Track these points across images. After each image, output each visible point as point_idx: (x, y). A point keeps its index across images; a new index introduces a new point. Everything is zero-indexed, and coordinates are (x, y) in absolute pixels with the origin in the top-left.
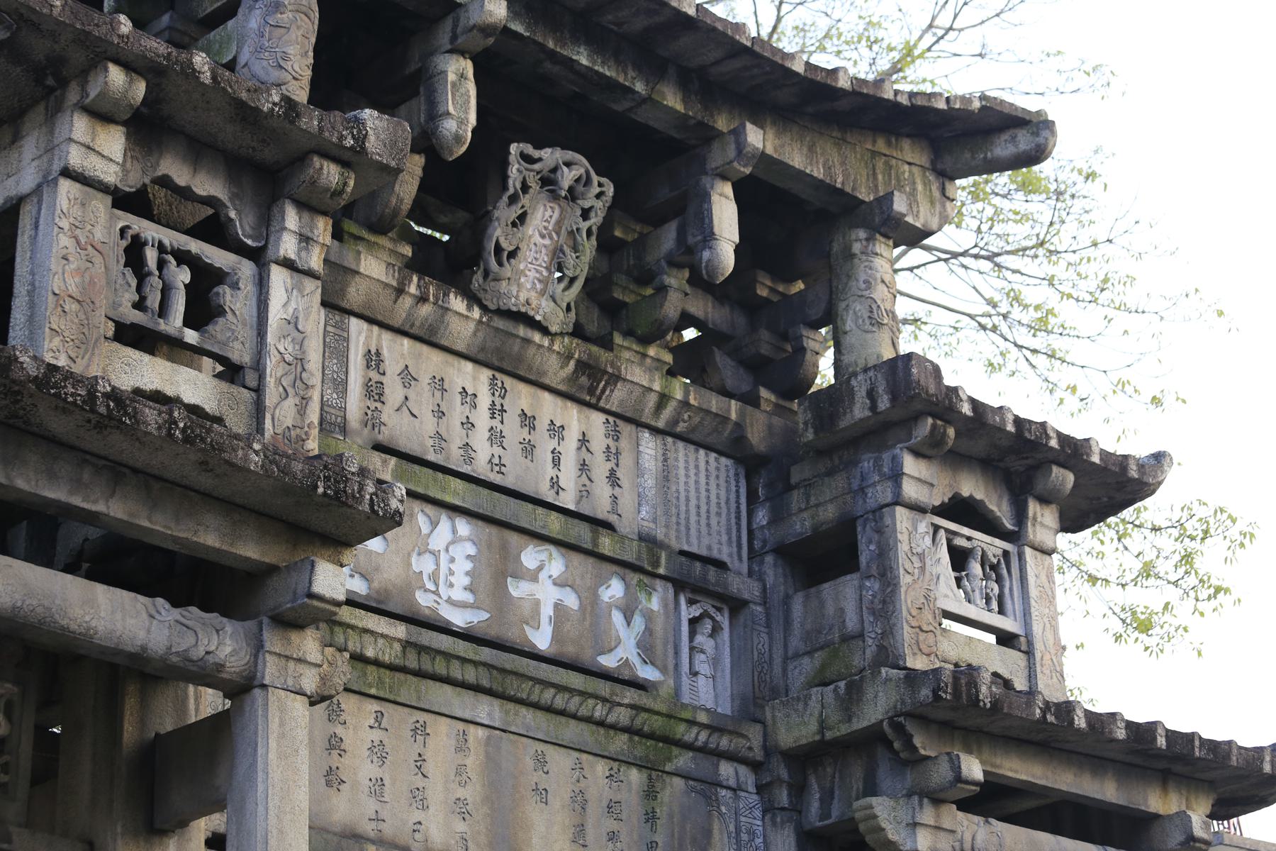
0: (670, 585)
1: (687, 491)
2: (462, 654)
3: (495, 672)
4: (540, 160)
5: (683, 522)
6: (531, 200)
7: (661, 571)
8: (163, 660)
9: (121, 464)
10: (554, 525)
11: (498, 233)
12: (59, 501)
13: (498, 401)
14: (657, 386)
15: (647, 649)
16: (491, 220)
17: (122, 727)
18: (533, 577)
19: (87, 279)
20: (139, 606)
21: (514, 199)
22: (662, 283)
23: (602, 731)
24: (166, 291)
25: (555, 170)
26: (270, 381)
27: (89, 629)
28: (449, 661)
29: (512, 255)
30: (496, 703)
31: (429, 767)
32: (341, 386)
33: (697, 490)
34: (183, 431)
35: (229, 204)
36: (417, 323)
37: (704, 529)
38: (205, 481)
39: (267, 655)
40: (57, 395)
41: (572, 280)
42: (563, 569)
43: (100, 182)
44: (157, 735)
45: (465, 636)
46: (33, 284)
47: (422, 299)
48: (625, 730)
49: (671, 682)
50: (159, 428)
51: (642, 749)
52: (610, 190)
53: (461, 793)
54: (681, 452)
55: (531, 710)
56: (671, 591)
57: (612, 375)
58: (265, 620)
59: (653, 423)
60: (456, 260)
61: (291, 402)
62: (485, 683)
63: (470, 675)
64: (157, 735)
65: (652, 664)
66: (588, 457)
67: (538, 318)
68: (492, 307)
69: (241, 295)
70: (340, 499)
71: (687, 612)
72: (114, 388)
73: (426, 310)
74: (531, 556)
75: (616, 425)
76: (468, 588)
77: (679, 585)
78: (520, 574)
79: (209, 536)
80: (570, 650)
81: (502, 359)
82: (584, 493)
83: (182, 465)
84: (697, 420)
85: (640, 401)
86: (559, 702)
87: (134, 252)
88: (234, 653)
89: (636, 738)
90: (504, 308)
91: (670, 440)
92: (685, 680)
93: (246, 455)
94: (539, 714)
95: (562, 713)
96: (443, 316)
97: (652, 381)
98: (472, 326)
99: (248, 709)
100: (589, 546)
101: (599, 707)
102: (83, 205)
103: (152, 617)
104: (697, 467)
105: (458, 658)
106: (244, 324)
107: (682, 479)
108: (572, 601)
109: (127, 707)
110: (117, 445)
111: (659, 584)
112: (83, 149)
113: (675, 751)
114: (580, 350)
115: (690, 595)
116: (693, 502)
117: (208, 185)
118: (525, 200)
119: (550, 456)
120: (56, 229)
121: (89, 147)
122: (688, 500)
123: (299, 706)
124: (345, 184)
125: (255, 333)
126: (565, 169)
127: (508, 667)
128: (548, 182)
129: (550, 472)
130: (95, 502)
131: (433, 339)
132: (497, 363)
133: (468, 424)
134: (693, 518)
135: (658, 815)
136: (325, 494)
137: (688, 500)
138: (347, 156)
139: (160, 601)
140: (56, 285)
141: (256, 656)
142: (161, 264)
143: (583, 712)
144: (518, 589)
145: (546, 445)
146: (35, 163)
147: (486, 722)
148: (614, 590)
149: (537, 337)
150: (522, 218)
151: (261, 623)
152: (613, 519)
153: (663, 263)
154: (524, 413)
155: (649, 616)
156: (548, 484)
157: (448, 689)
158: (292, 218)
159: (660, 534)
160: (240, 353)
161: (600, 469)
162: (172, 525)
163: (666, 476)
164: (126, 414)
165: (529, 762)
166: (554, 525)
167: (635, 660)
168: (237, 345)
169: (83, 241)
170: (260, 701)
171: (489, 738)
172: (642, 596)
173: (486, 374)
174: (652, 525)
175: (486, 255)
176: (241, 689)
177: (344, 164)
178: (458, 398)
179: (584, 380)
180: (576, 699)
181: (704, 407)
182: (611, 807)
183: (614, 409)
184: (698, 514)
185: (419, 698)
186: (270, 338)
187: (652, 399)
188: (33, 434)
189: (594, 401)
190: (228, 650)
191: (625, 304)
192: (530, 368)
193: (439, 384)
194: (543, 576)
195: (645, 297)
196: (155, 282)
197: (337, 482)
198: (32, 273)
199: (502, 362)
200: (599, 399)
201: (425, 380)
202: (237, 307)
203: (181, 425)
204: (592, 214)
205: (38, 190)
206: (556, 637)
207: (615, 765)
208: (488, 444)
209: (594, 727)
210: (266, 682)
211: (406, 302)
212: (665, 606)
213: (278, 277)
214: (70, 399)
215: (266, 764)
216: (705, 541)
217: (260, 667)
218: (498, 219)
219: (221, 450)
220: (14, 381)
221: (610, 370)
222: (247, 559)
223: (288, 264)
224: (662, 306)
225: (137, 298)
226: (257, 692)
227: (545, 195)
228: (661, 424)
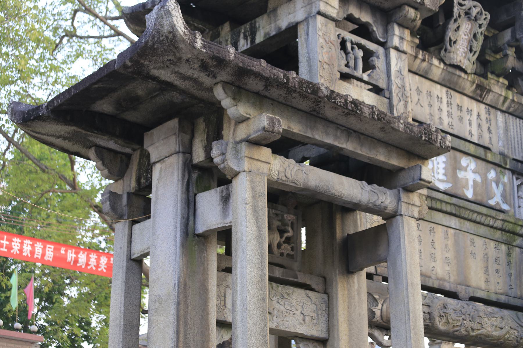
0: (510, 172)
1: (514, 135)
2: (446, 200)
3: (457, 207)
4: (465, 5)
5: (513, 147)
6: (461, 21)
7: (508, 167)
8: (366, 206)
9: (350, 129)
10: (472, 149)
11: (450, 34)
12: (330, 144)
13: (449, 100)
14: (503, 94)
15: (504, 196)
16: (447, 29)
17: (336, 231)
18: (465, 169)
19: (330, 55)
20: (357, 184)
21: (456, 20)
22: (506, 53)
23: (492, 230)
24: (356, 59)
25: (470, 9)
26: (394, 95)
27: (341, 194)
28: (441, 203)
29: (455, 42)
30: (457, 219)
31: (436, 245)
33: (517, 134)
34: (377, 116)
35: (373, 25)
36: (421, 70)
37: (520, 150)
38: (380, 135)
39: (402, 203)
40: (335, 102)
41: (475, 52)
42: (475, 166)
43: (331, 17)
44: (348, 234)
45: (445, 193)
46: (309, 57)
47: (424, 60)
48: (500, 229)
49: (513, 210)
50: (369, 115)
51: (506, 237)
52: (489, 17)
53: (447, 255)
54: (511, 119)
55: (469, 222)
56: (511, 174)
57: (488, 90)
58: (401, 189)
59: (501, 108)
61: (402, 103)
62: (454, 212)
63: (448, 208)
64: (348, 234)
65: (506, 203)
66: (480, 122)
67: (464, 67)
68: (448, 63)
69: (380, 60)
70: (430, 142)
71: (516, 183)
72: (353, 99)
73: (425, 64)
74: (465, 161)
75: (489, 109)
76: (445, 174)
77: (513, 172)
78: (461, 168)
79: (381, 156)
80: (479, 198)
81: (450, 84)
82: (480, 137)
83: (374, 129)
84: (517, 107)
85: (498, 100)
86: (478, 219)
87: (343, 44)
88: (391, 202)
89: (503, 233)
90: (452, 63)
91: (507, 115)
92: (517, 209)
93: (398, 125)
94: (472, 224)
95: (479, 223)
96: (430, 67)
97: (502, 92)
98: (440, 71)
99: (394, 224)
100: (483, 157)
101: (491, 220)
102: (326, 26)
103: (362, 188)
104: (516, 125)
105: (445, 202)
106: (382, 72)
107: (512, 130)
108: (479, 179)
109: (337, 223)
110: (352, 122)
111: (507, 172)
112: (325, 4)
113: (516, 237)
114: (478, 80)
115: (517, 176)
116: (516, 139)
117: (365, 17)
118: (459, 21)
119: (468, 122)
120: (318, 36)
121: (327, 3)
122: (514, 138)
123: (413, 223)
124: (417, 17)
125: (386, 76)
126: (474, 8)
127: (461, 205)
128: (467, 13)
129: (468, 128)
130: (342, 144)
131: (427, 76)
132: (448, 85)
133: (440, 110)
134: (516, 146)
135: (512, 262)
136: (425, 140)
137: (514, 138)
138: (417, 6)
139: (364, 182)
140: (320, 58)
141: (398, 203)
142: (353, 49)
143: (486, 222)
144: (461, 175)
145: (466, 117)
146: (303, 9)
147: (454, 227)
148: (492, 174)
149: (463, 75)
150: (458, 28)
151: (399, 190)
152: (490, 146)
153: (506, 45)
154: (458, 105)
155: (504, 185)
156: (468, 133)
157: (441, 214)
158: (397, 30)
159: (506, 152)
160: (382, 84)
161: (485, 127)
162: (369, 152)
163: (506, 129)
164: (358, 109)
165: (469, 243)
166: (472, 149)
167: (501, 202)
168: (381, 81)
169: (327, 40)
170: (400, 221)
171: (455, 233)
172: (501, 177)
173: (444, 89)
174: (503, 149)
175: (446, 43)
176: (390, 217)
177: (416, 9)
178: (436, 99)
179: (479, 92)
180: (484, 218)
181: (520, 102)
182: (497, 259)
183: (488, 103)
184: (518, 144)
185: (431, 218)
186: (393, 78)
187: (502, 99)
188: (319, 117)
189: (481, 100)
190: (389, 201)
191: (489, 61)
192: (460, 87)
193: (430, 94)
194: (468, 169)
195: (497, 59)
196: (351, 56)
197: (429, 135)
198: (308, 53)
199: (450, 85)
200: (483, 99)
201: (425, 92)
202: (379, 65)
203: (376, 113)
204: (483, 26)
205: (306, 19)
206: (475, 193)
207: (497, 243)
208: (447, 117)
209: (489, 228)
210: (402, 213)
211: (418, 61)
212: (509, 180)
213: (393, 53)
214: (339, 104)
215: (405, 245)
216: (521, 155)
217: (399, 208)
218: (450, 28)
219: (390, 123)
220: (320, 97)
221: (488, 88)
222: (394, 165)
223: (396, 49)
224: (506, 62)
225: (346, 62)
226: (398, 217)
227: (466, 19)
228: (504, 109)
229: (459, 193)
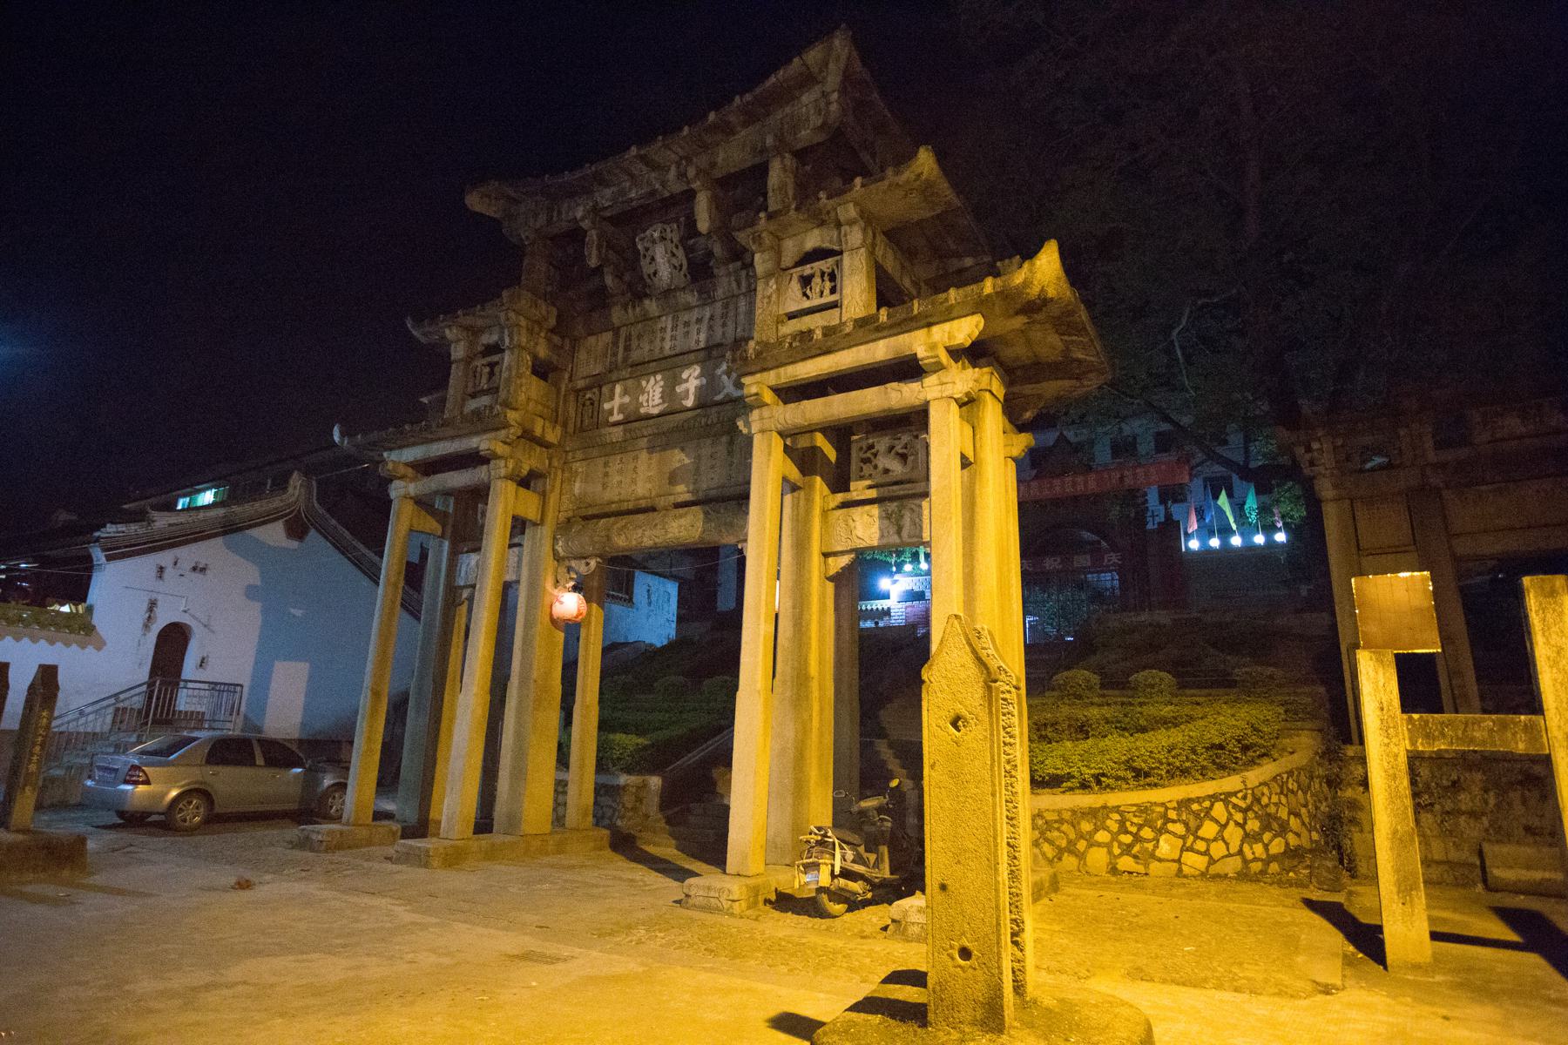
18: (687, 381)
32: (615, 355)
45: (659, 416)
60: (639, 289)
128: (654, 242)
150: (653, 259)
229: (678, 407)
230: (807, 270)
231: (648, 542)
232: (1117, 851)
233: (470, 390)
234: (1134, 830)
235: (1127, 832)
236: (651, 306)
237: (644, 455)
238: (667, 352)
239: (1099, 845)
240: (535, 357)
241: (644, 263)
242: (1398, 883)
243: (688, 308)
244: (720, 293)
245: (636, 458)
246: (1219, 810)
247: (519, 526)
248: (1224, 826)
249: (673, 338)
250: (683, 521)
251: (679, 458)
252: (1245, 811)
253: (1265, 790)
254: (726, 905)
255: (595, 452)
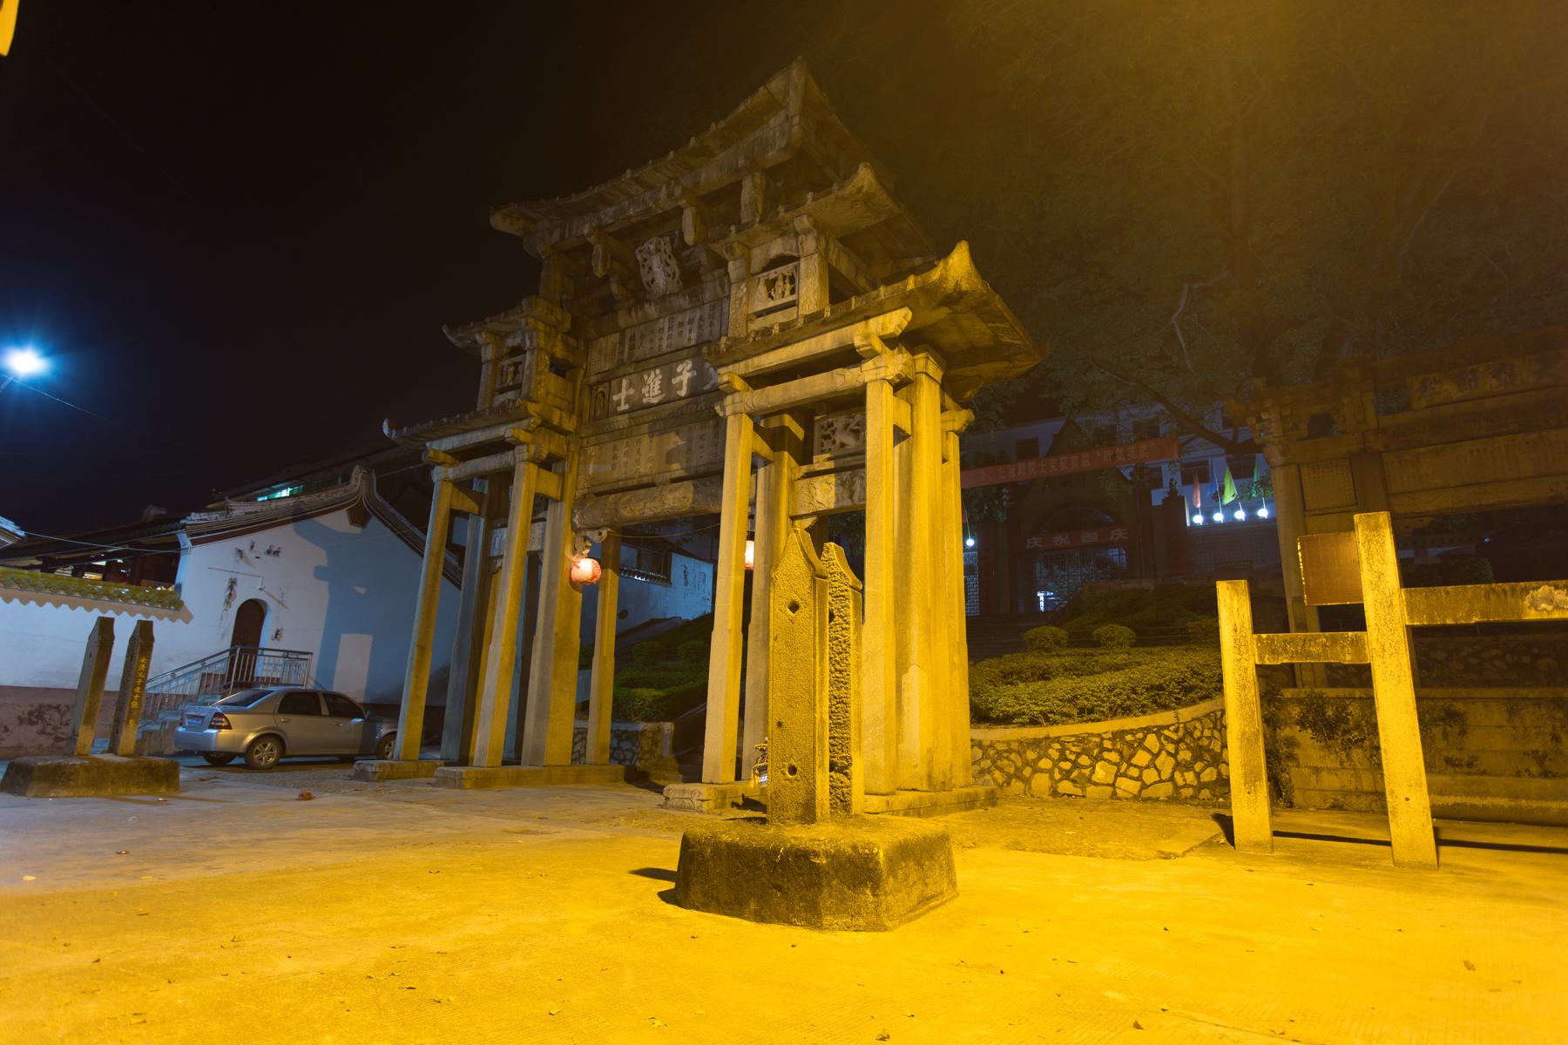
32: (622, 352)
60: (639, 294)
128: (650, 253)
230: (772, 274)
231: (648, 513)
232: (1057, 776)
233: (498, 386)
234: (1073, 757)
235: (1067, 760)
236: (651, 310)
237: (646, 439)
238: (665, 349)
239: (1042, 771)
240: (553, 357)
241: (643, 272)
242: (1245, 776)
243: (682, 311)
244: (707, 296)
245: (639, 441)
246: (1152, 741)
247: (541, 503)
248: (1156, 756)
249: (670, 337)
250: (677, 494)
251: (675, 441)
252: (1177, 743)
253: (1198, 725)
254: (697, 804)
255: (606, 437)
